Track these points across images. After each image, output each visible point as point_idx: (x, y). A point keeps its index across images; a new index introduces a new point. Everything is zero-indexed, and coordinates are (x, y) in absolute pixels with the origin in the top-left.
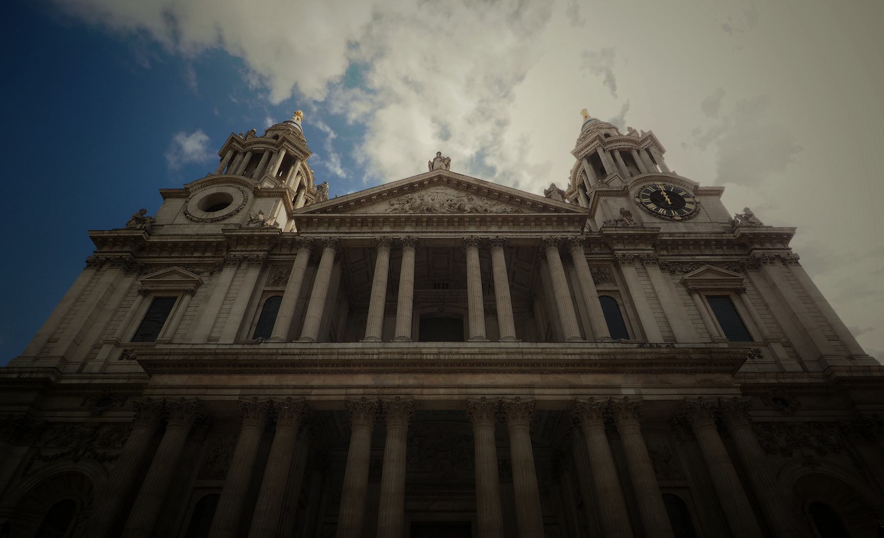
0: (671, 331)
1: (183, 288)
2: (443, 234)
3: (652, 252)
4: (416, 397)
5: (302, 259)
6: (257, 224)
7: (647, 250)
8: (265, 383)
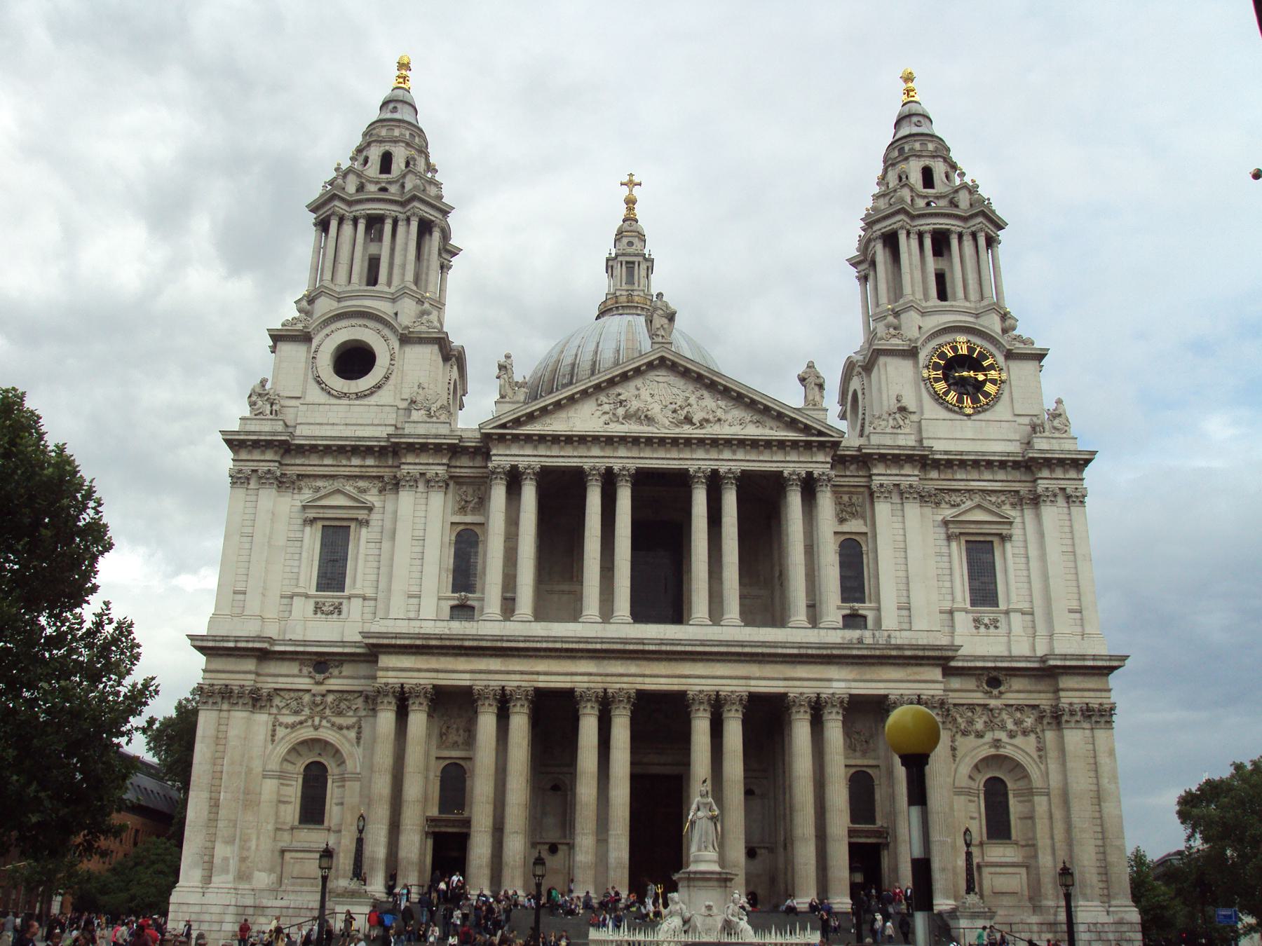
0: (908, 597)
1: (354, 516)
2: (665, 462)
3: (917, 479)
4: (639, 687)
5: (498, 494)
6: (423, 412)
7: (910, 476)
8: (493, 667)
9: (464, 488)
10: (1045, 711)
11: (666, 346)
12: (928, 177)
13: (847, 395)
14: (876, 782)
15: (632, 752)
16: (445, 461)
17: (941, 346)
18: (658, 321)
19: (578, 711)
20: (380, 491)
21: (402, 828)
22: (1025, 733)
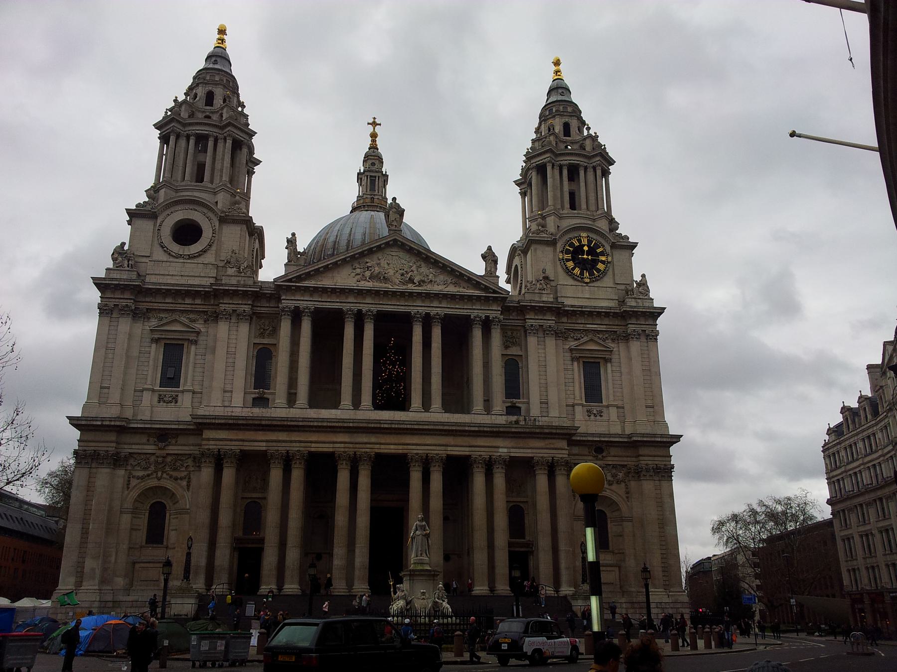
2: (396, 307)
3: (554, 322)
4: (377, 451)
6: (235, 269)
7: (550, 321)
8: (281, 439)
9: (263, 321)
10: (630, 469)
11: (398, 232)
12: (567, 128)
13: (512, 268)
14: (526, 512)
15: (372, 493)
16: (249, 302)
17: (571, 239)
18: (392, 216)
19: (337, 466)
20: (205, 321)
21: (217, 545)
22: (618, 482)
